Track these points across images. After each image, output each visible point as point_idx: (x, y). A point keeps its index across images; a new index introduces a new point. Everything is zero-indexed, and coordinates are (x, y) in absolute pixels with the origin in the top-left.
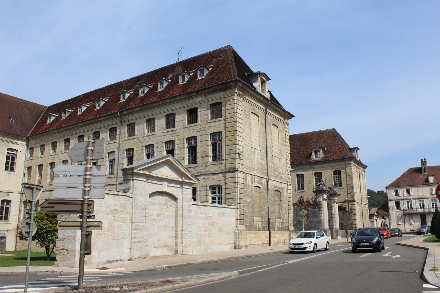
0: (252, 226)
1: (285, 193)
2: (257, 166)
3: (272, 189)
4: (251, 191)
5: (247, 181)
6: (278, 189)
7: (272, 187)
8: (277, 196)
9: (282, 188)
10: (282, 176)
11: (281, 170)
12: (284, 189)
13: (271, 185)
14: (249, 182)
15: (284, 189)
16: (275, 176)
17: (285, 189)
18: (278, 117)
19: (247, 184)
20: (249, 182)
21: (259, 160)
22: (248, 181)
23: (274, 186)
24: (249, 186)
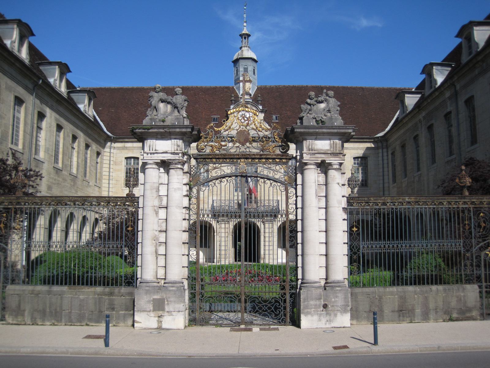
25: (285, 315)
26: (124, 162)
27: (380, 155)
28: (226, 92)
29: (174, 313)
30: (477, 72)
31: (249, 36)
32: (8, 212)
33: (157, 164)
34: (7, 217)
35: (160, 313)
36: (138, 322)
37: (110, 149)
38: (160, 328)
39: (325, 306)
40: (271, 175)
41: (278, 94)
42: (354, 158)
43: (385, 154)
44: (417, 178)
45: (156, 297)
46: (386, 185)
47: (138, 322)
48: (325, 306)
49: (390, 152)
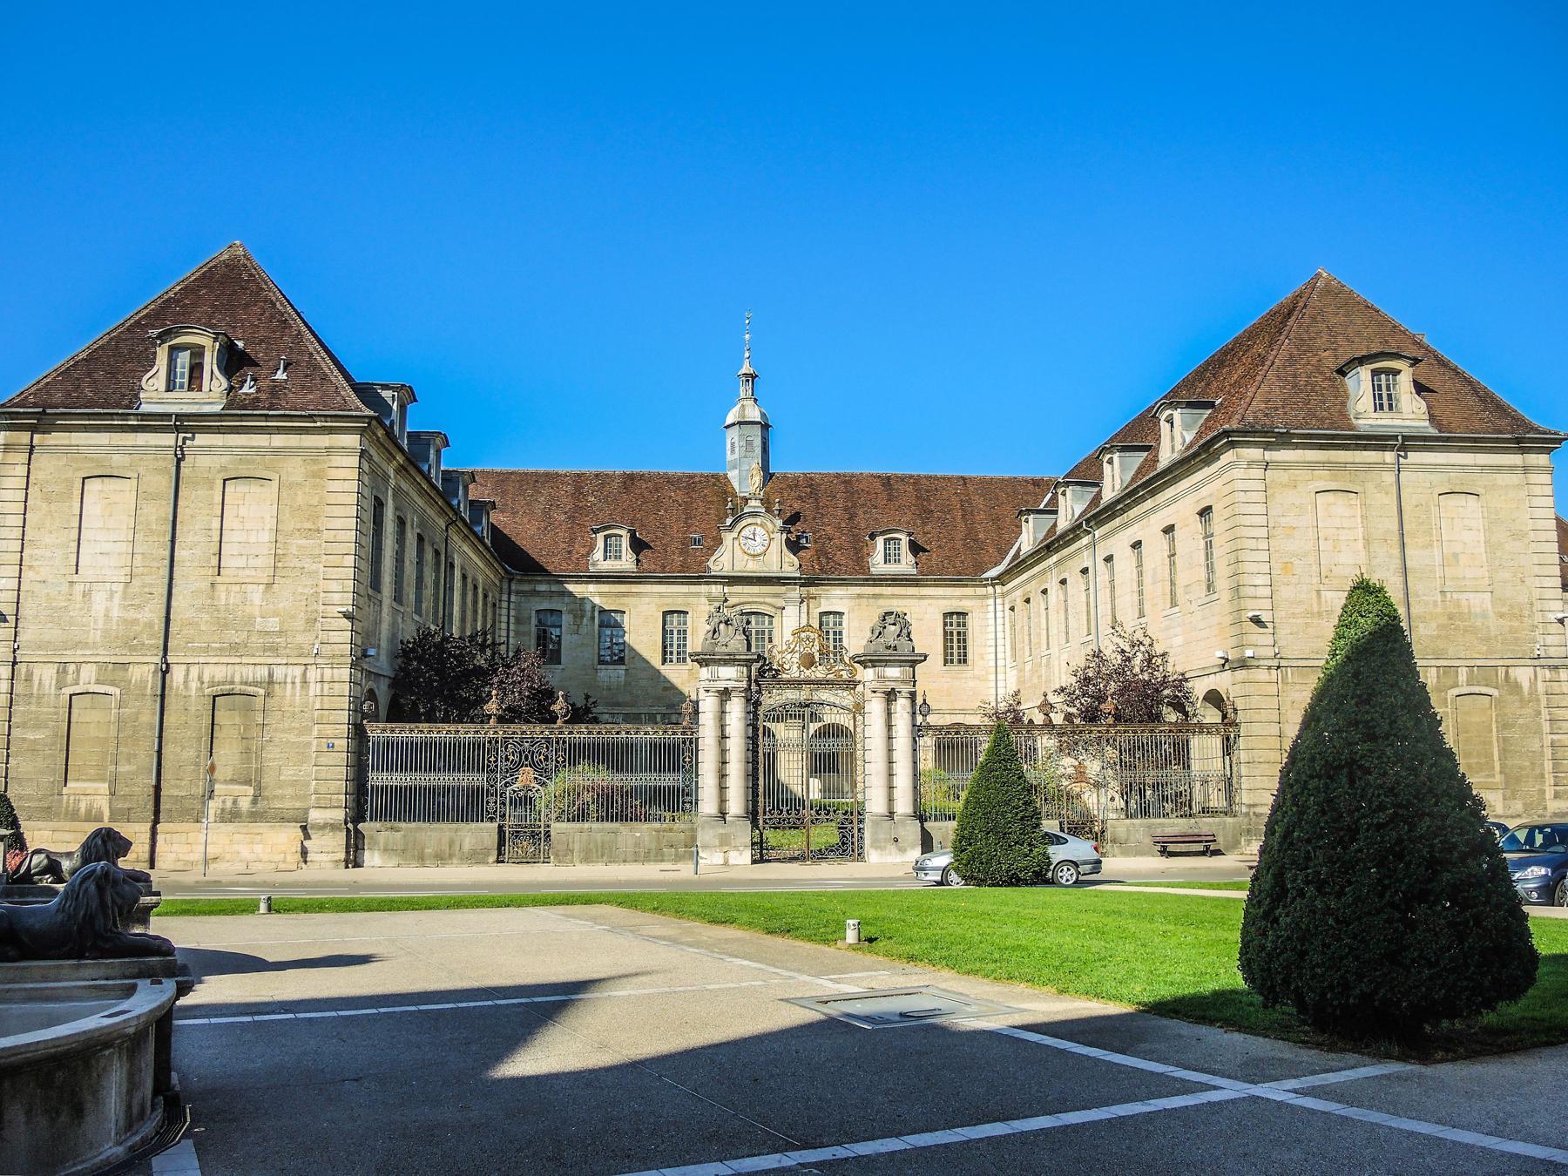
0: (49, 808)
1: (294, 695)
2: (99, 632)
3: (193, 693)
4: (52, 710)
5: (36, 683)
6: (239, 687)
7: (194, 685)
8: (237, 713)
9: (271, 682)
10: (278, 640)
11: (273, 624)
12: (289, 686)
13: (186, 682)
14: (47, 683)
15: (289, 686)
16: (221, 649)
17: (293, 683)
18: (279, 440)
19: (35, 691)
20: (47, 683)
21: (116, 613)
22: (40, 683)
23: (206, 678)
24: (40, 697)
25: (853, 851)
26: (534, 621)
27: (991, 608)
28: (714, 485)
29: (741, 848)
30: (1117, 521)
31: (754, 377)
32: (549, 742)
33: (718, 692)
34: (547, 748)
35: (726, 849)
36: (702, 858)
37: (509, 595)
38: (726, 864)
39: (896, 840)
40: (837, 702)
41: (809, 490)
42: (945, 615)
43: (999, 608)
44: (1044, 660)
45: (722, 831)
46: (1000, 663)
47: (702, 858)
48: (896, 840)
49: (1007, 607)
